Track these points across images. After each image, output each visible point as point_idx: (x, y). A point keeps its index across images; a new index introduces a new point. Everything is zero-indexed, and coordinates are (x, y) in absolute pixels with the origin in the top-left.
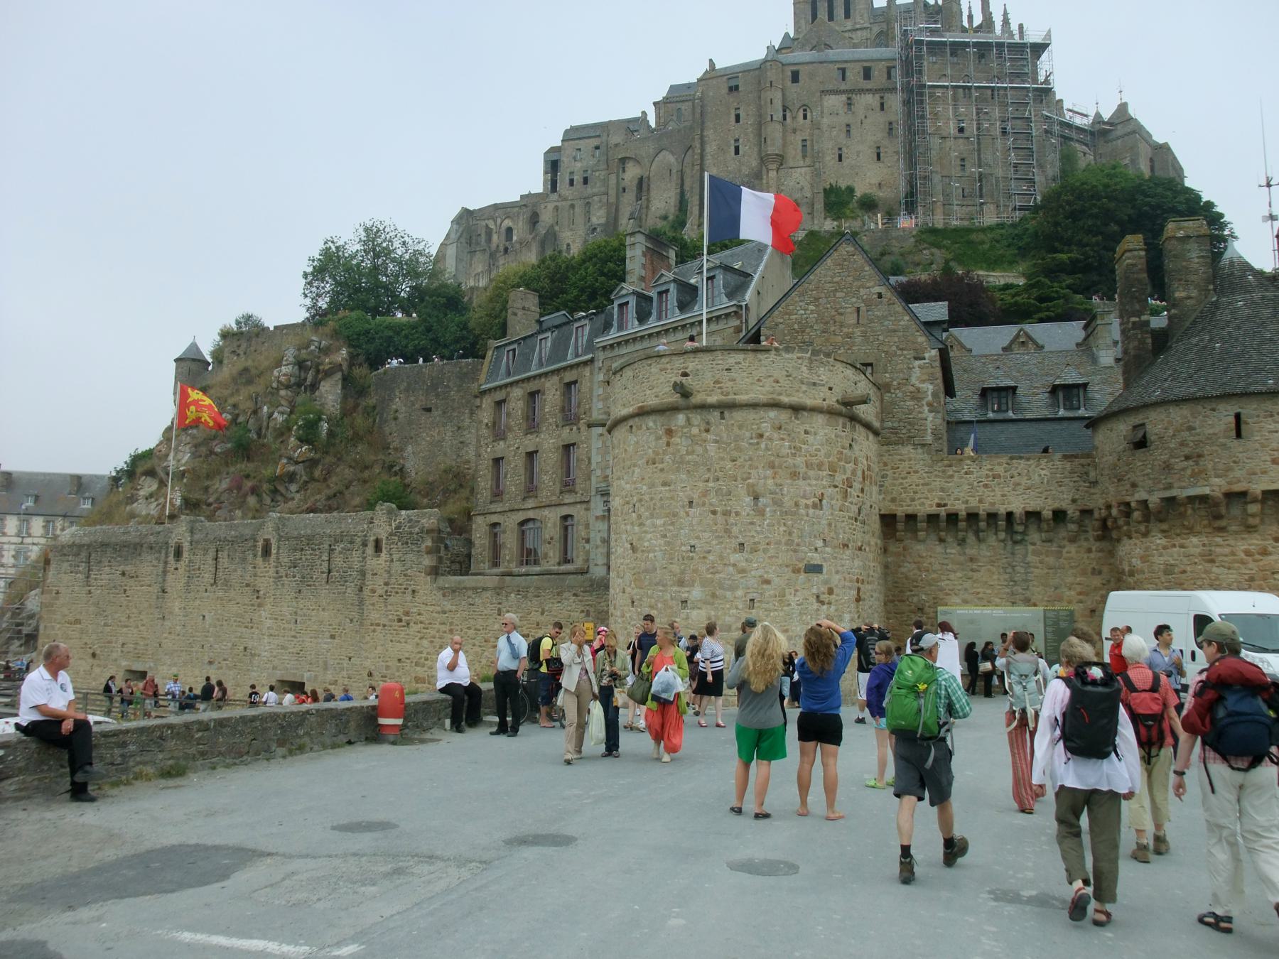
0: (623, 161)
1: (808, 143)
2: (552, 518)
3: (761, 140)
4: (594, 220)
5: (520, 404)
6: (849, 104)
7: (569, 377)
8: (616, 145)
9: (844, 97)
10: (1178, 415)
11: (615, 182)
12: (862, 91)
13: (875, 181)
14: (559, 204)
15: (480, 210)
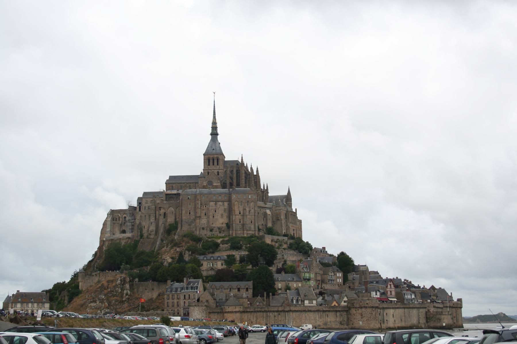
0: (160, 208)
1: (206, 213)
2: (176, 310)
3: (196, 212)
4: (151, 220)
5: (171, 296)
6: (216, 204)
7: (178, 294)
8: (158, 203)
9: (214, 203)
10: (226, 306)
11: (158, 213)
12: (219, 201)
13: (221, 222)
14: (142, 215)
15: (116, 210)
